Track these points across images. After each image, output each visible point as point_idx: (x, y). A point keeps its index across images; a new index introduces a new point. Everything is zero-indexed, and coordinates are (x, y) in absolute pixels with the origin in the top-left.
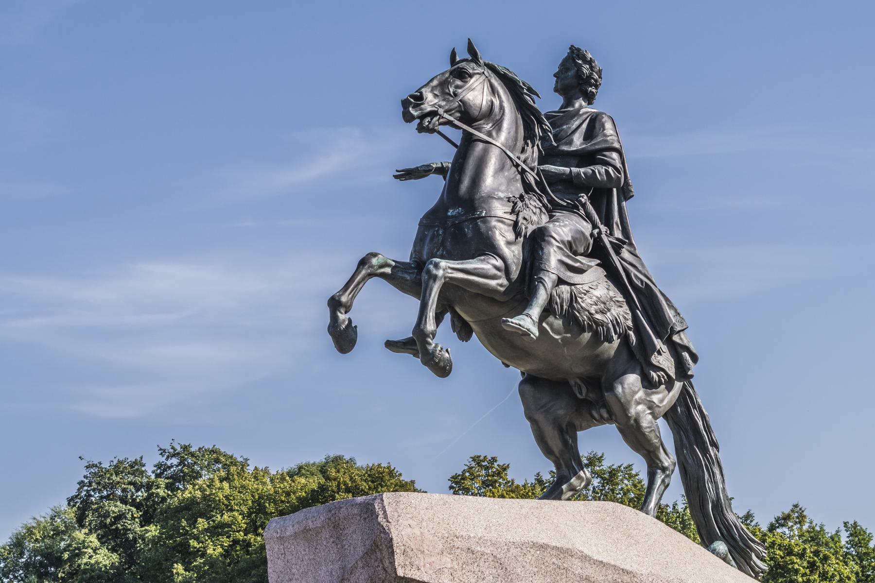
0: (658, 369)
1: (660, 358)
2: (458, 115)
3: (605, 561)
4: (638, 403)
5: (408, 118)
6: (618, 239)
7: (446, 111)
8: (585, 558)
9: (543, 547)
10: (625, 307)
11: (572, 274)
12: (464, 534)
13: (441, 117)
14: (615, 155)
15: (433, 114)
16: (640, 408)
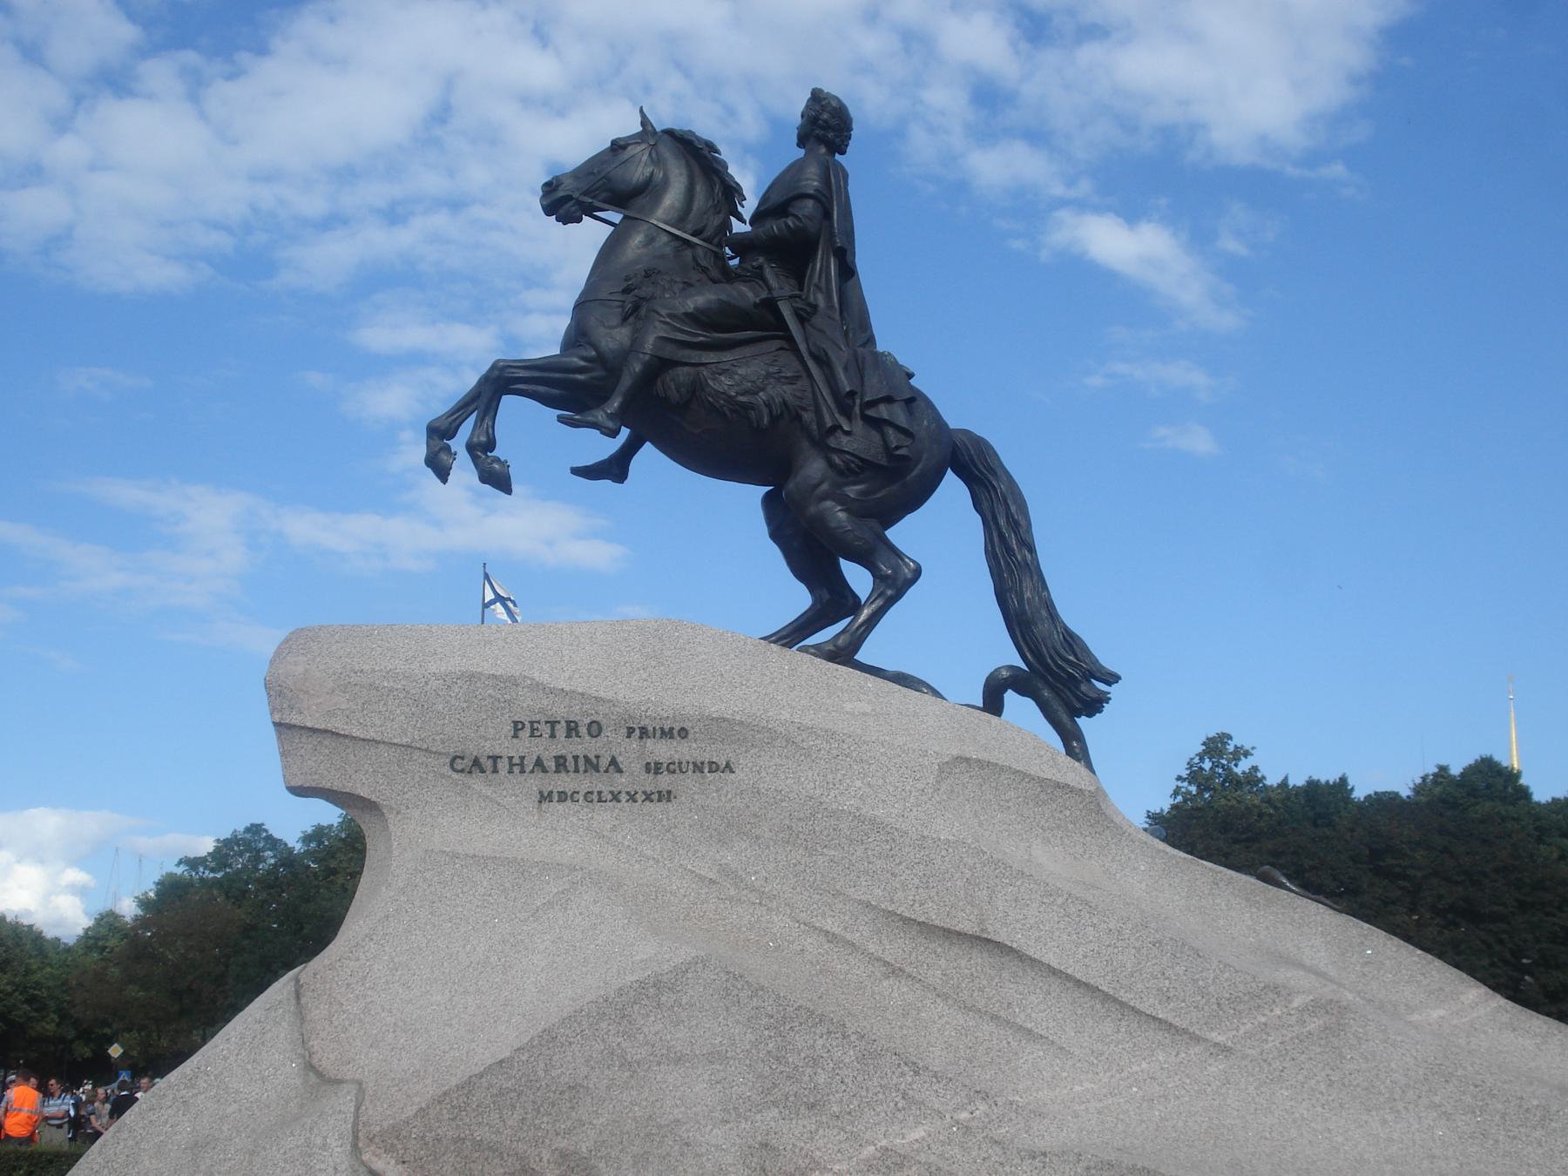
0: (840, 451)
1: (844, 439)
2: (604, 195)
3: (567, 689)
4: (823, 498)
5: (549, 210)
6: (810, 305)
7: (585, 194)
8: (537, 686)
9: (472, 677)
10: (803, 383)
11: (687, 352)
12: (366, 667)
13: (579, 203)
14: (810, 203)
15: (568, 198)
16: (829, 503)
